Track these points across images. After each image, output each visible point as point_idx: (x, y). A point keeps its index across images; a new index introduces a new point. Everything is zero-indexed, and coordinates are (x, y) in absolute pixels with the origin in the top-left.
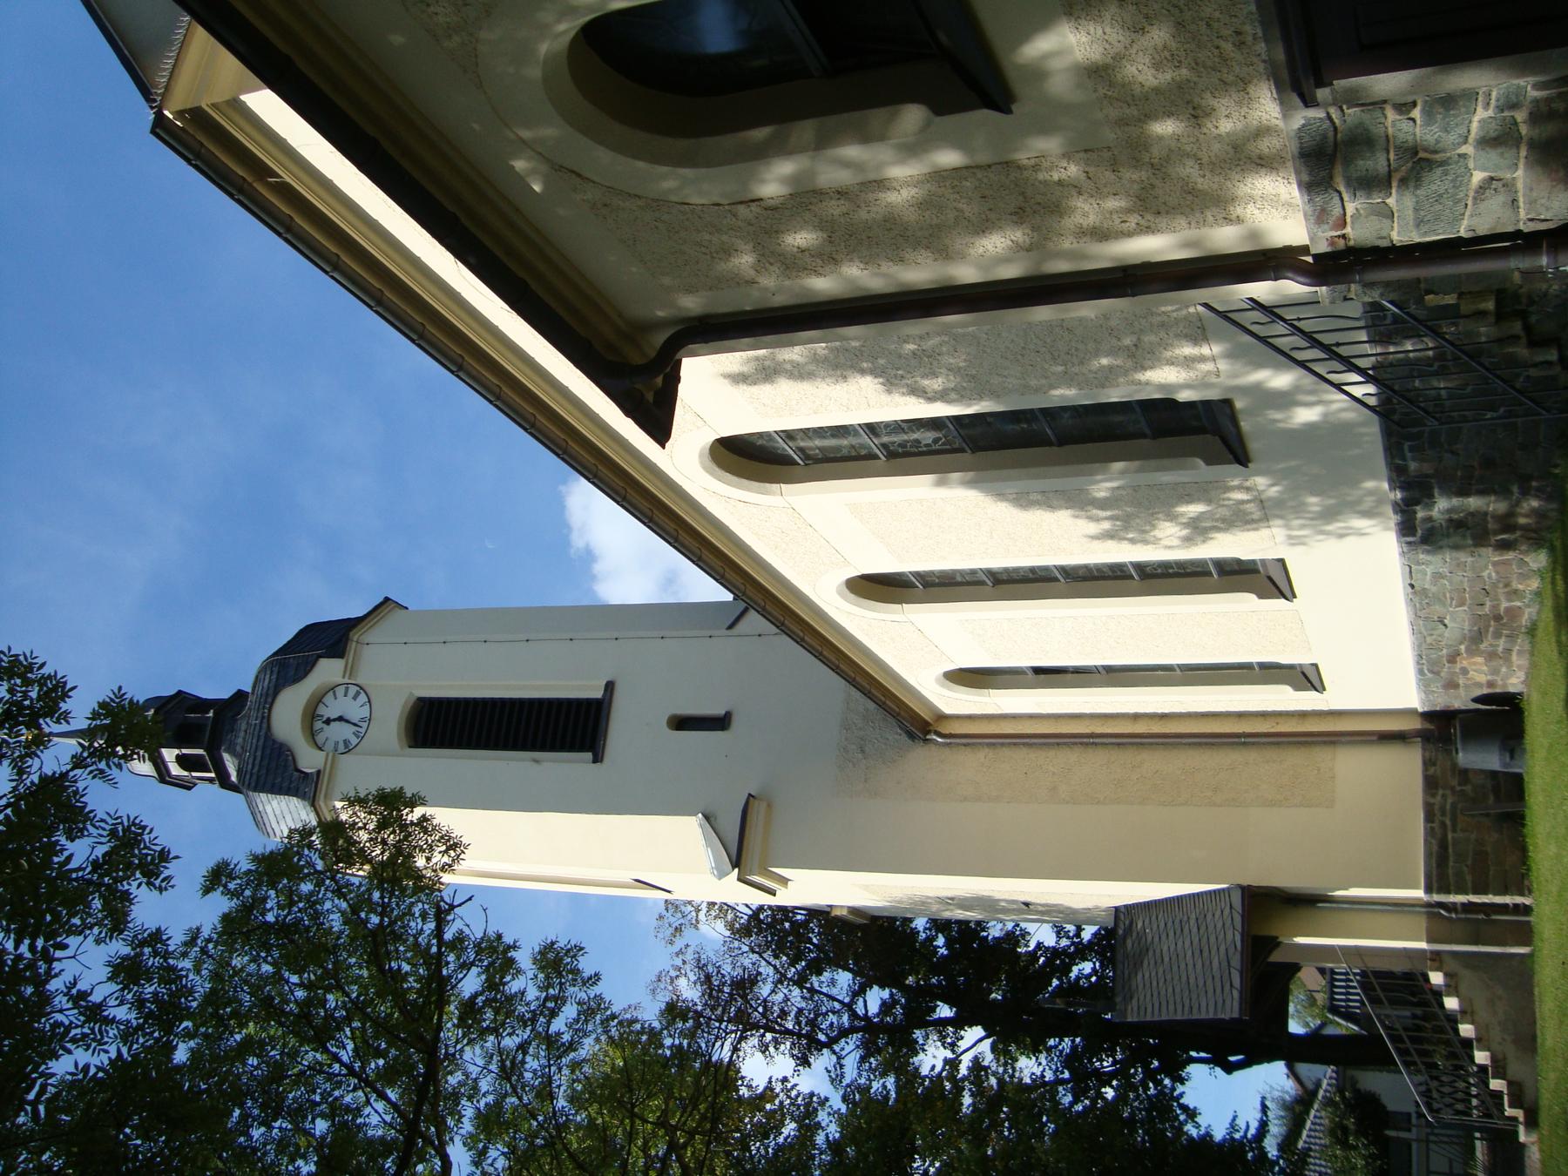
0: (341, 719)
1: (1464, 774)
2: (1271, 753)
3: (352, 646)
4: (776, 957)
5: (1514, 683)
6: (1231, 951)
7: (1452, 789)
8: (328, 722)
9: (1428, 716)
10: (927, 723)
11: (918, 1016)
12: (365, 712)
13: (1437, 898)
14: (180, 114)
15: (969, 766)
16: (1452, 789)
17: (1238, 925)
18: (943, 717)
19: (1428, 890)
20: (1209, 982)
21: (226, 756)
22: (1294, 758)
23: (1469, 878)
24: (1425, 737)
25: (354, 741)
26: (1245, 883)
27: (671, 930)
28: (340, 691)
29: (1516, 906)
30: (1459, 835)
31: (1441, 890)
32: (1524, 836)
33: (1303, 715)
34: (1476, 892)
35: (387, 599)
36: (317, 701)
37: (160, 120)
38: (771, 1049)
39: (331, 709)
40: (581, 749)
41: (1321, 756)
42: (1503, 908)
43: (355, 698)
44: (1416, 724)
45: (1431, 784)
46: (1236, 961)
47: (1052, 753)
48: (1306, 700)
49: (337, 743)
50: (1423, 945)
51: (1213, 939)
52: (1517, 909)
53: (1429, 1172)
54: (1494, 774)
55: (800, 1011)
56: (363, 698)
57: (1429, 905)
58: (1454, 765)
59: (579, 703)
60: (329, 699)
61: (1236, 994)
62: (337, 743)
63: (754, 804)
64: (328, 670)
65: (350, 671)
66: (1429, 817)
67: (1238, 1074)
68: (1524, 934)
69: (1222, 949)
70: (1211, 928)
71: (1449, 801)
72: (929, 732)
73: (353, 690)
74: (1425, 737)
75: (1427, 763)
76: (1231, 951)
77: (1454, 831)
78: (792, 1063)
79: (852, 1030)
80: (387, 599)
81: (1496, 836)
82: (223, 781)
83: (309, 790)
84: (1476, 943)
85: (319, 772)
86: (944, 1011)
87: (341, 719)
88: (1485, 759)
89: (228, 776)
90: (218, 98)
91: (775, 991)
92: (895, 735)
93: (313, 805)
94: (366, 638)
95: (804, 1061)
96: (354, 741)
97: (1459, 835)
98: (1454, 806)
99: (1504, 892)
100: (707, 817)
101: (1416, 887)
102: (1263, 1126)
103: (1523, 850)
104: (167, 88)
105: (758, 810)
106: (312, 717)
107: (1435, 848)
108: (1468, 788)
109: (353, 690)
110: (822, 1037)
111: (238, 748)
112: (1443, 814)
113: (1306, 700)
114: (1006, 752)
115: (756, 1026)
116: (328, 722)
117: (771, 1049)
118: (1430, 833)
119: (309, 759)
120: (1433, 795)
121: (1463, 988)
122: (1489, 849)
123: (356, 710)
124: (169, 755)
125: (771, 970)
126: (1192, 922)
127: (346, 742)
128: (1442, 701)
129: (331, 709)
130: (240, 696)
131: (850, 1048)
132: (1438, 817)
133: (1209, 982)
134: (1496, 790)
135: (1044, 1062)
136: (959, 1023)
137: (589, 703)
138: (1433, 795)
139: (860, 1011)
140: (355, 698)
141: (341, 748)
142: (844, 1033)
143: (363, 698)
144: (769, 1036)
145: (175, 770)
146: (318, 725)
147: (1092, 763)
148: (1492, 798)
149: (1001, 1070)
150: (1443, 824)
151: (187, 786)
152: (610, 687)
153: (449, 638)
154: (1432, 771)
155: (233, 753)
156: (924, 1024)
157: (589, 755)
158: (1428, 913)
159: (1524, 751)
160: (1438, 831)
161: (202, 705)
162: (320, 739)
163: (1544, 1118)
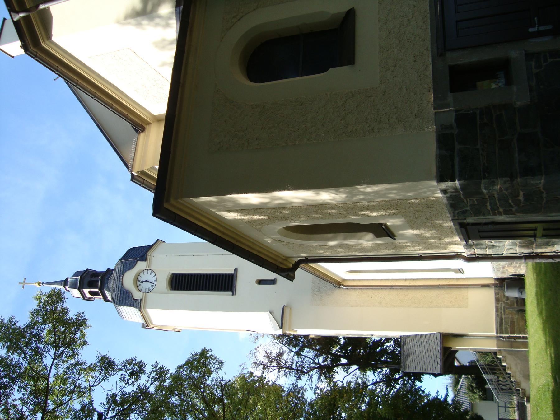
0: (146, 281)
1: (507, 298)
2: (448, 291)
3: (148, 257)
4: (289, 346)
5: (522, 272)
6: (437, 352)
7: (504, 302)
8: (142, 282)
9: (497, 279)
10: (340, 282)
11: (335, 361)
12: (154, 279)
13: (499, 335)
14: (137, 172)
15: (354, 295)
16: (504, 302)
17: (439, 343)
18: (344, 280)
19: (497, 333)
20: (431, 362)
21: (106, 292)
22: (455, 293)
23: (509, 329)
24: (496, 286)
25: (152, 288)
26: (441, 332)
27: (255, 339)
28: (145, 272)
29: (523, 337)
30: (506, 316)
31: (500, 333)
32: (525, 317)
33: (458, 279)
34: (511, 334)
35: (158, 240)
36: (138, 275)
37: (133, 176)
38: (288, 375)
39: (143, 278)
40: (228, 290)
41: (464, 292)
42: (520, 338)
43: (151, 274)
44: (493, 282)
45: (497, 300)
46: (439, 356)
47: (380, 291)
48: (459, 275)
49: (146, 289)
50: (496, 348)
51: (431, 349)
52: (524, 338)
53: (499, 419)
54: (516, 298)
55: (297, 362)
56: (153, 274)
57: (497, 337)
58: (504, 295)
59: (226, 275)
60: (142, 274)
61: (439, 366)
62: (146, 289)
63: (286, 309)
64: (141, 265)
65: (149, 265)
66: (497, 311)
67: (438, 378)
68: (526, 345)
69: (435, 352)
70: (431, 345)
71: (503, 305)
72: (340, 285)
73: (150, 271)
74: (496, 286)
75: (496, 294)
76: (437, 352)
77: (504, 315)
78: (295, 378)
79: (314, 368)
80: (158, 240)
81: (517, 316)
82: (106, 299)
83: (138, 305)
84: (512, 348)
85: (141, 300)
86: (344, 361)
87: (146, 281)
88: (513, 294)
89: (107, 297)
90: (148, 167)
91: (289, 356)
92: (330, 286)
93: (140, 310)
94: (153, 254)
95: (299, 378)
96: (152, 288)
97: (506, 316)
98: (504, 307)
99: (520, 333)
100: (271, 313)
101: (493, 332)
102: (447, 395)
103: (525, 321)
104: (133, 165)
105: (287, 311)
106: (137, 281)
107: (499, 320)
108: (509, 301)
109: (150, 271)
110: (305, 371)
111: (110, 289)
112: (501, 309)
113: (459, 275)
114: (365, 291)
115: (282, 367)
116: (142, 282)
117: (288, 375)
118: (497, 315)
119: (137, 295)
120: (498, 304)
121: (508, 361)
122: (515, 320)
123: (151, 278)
124: (86, 291)
125: (287, 349)
126: (425, 342)
127: (149, 289)
128: (500, 276)
129: (143, 278)
130: (109, 271)
131: (315, 374)
132: (500, 311)
133: (431, 362)
134: (517, 302)
135: (377, 377)
136: (348, 365)
137: (229, 275)
138: (498, 304)
139: (317, 361)
140: (151, 274)
141: (147, 291)
142: (312, 369)
143: (153, 274)
144: (287, 370)
145: (88, 296)
146: (139, 283)
147: (393, 294)
148: (516, 304)
149: (362, 376)
150: (501, 313)
151: (92, 300)
152: (236, 270)
153: (181, 254)
154: (497, 296)
155: (109, 290)
156: (337, 366)
157: (231, 292)
158: (498, 340)
159: (525, 292)
160: (500, 315)
161: (96, 274)
162: (140, 288)
163: (531, 399)
